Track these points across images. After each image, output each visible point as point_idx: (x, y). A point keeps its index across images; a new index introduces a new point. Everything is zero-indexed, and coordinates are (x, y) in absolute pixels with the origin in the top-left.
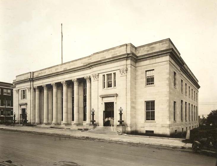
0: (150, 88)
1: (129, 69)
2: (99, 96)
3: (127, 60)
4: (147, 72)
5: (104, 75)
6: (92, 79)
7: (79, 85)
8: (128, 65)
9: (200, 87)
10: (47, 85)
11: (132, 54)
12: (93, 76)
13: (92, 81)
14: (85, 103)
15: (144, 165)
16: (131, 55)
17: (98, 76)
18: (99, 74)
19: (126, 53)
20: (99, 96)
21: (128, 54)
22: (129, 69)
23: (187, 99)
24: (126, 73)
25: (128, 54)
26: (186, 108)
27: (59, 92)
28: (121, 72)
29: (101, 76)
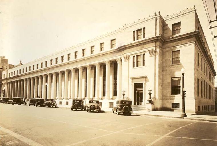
0: (65, 103)
1: (158, 50)
2: (129, 78)
3: (156, 42)
4: (174, 53)
5: (134, 57)
6: (123, 59)
7: (19, 81)
8: (157, 46)
9: (179, 103)
10: (61, 72)
11: (161, 37)
12: (124, 57)
13: (122, 61)
14: (115, 86)
15: (186, 145)
16: (160, 38)
17: (129, 57)
18: (129, 55)
19: (155, 36)
20: (129, 78)
21: (157, 37)
22: (158, 50)
23: (207, 80)
24: (154, 53)
25: (157, 36)
26: (208, 87)
27: (77, 76)
28: (151, 53)
29: (131, 57)
